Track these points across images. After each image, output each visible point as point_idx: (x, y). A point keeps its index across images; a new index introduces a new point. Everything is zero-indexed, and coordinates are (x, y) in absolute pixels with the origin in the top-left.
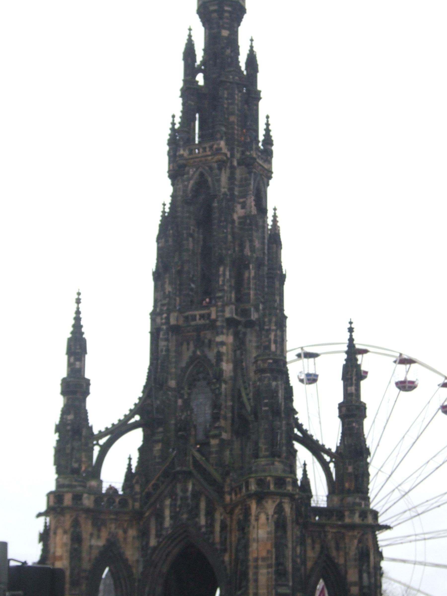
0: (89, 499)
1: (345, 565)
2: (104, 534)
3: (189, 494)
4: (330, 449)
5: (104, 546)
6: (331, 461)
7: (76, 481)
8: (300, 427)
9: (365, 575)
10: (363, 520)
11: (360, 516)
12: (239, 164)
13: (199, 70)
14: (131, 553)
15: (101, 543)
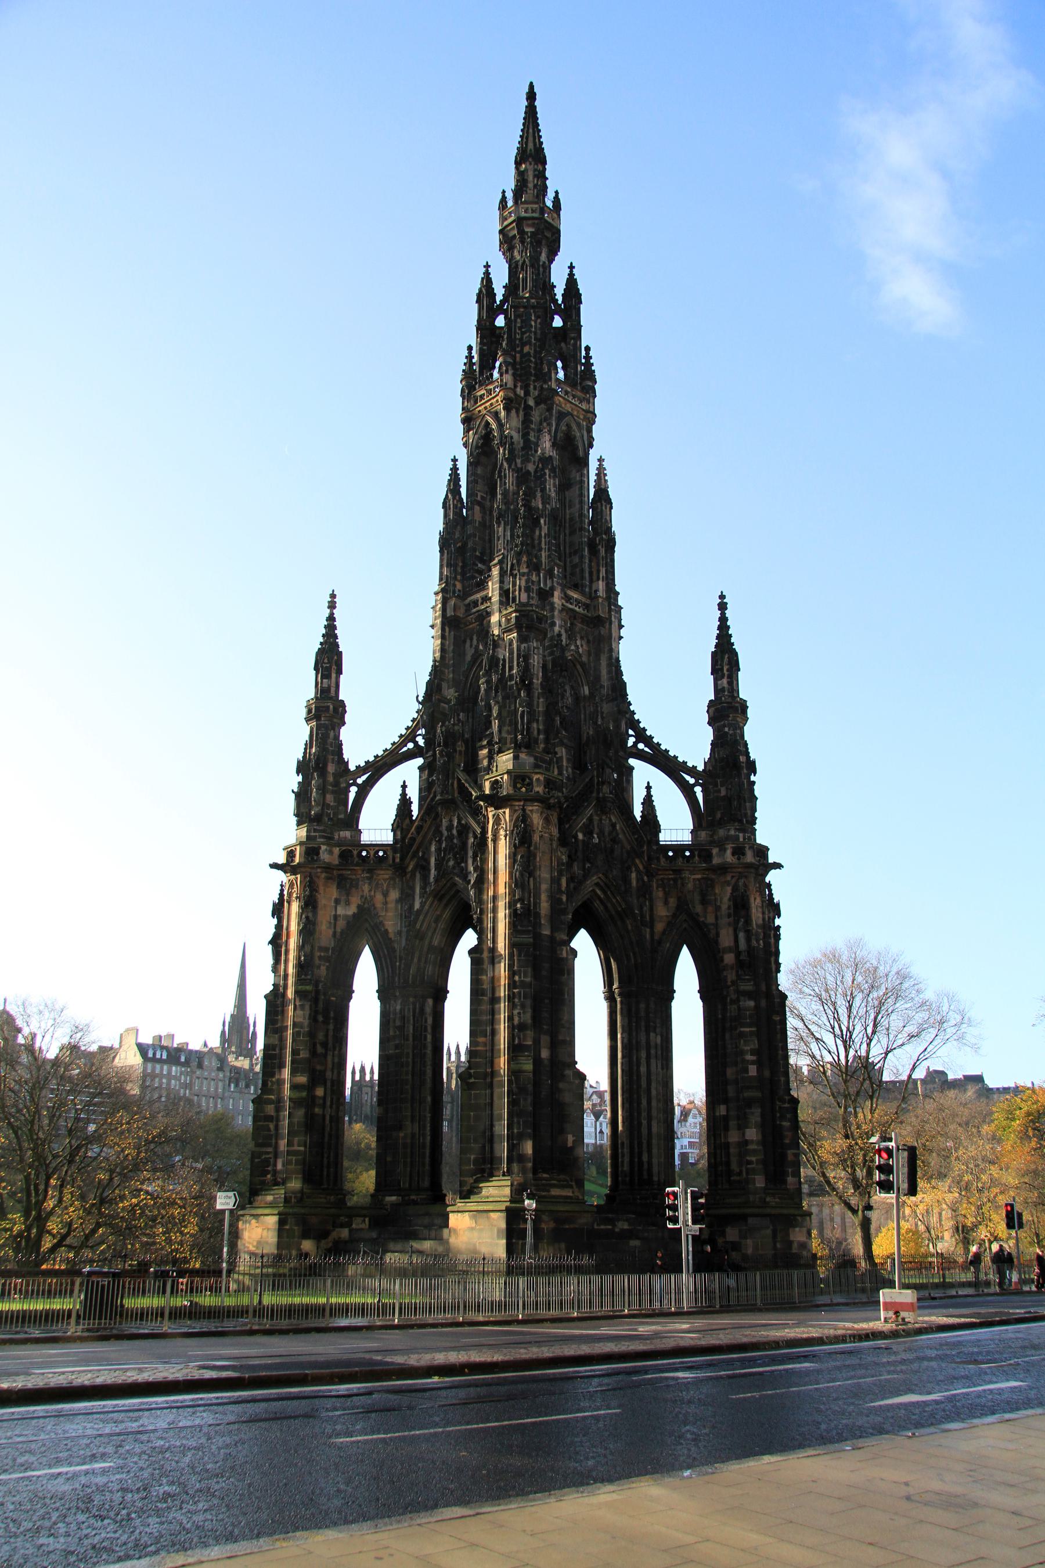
0: (331, 852)
1: (716, 925)
2: (355, 901)
3: (455, 832)
4: (694, 767)
5: (354, 915)
6: (696, 784)
7: (315, 831)
8: (648, 740)
9: (741, 935)
10: (739, 859)
11: (733, 854)
12: (537, 404)
13: (500, 310)
14: (391, 923)
15: (352, 910)
